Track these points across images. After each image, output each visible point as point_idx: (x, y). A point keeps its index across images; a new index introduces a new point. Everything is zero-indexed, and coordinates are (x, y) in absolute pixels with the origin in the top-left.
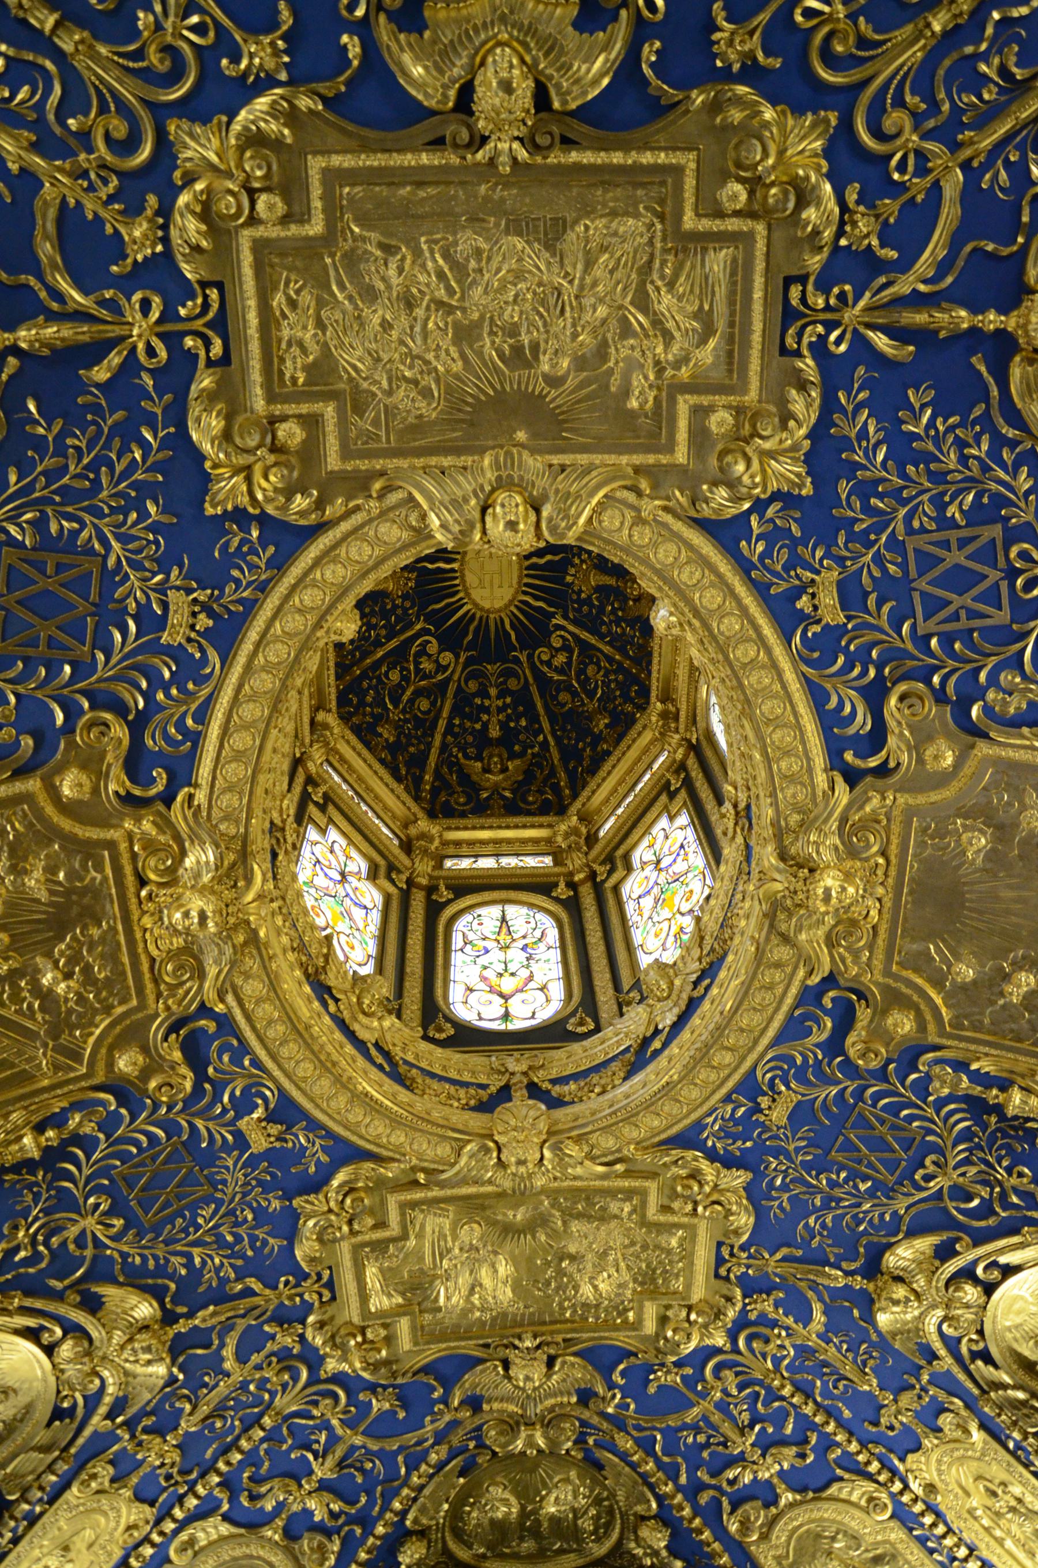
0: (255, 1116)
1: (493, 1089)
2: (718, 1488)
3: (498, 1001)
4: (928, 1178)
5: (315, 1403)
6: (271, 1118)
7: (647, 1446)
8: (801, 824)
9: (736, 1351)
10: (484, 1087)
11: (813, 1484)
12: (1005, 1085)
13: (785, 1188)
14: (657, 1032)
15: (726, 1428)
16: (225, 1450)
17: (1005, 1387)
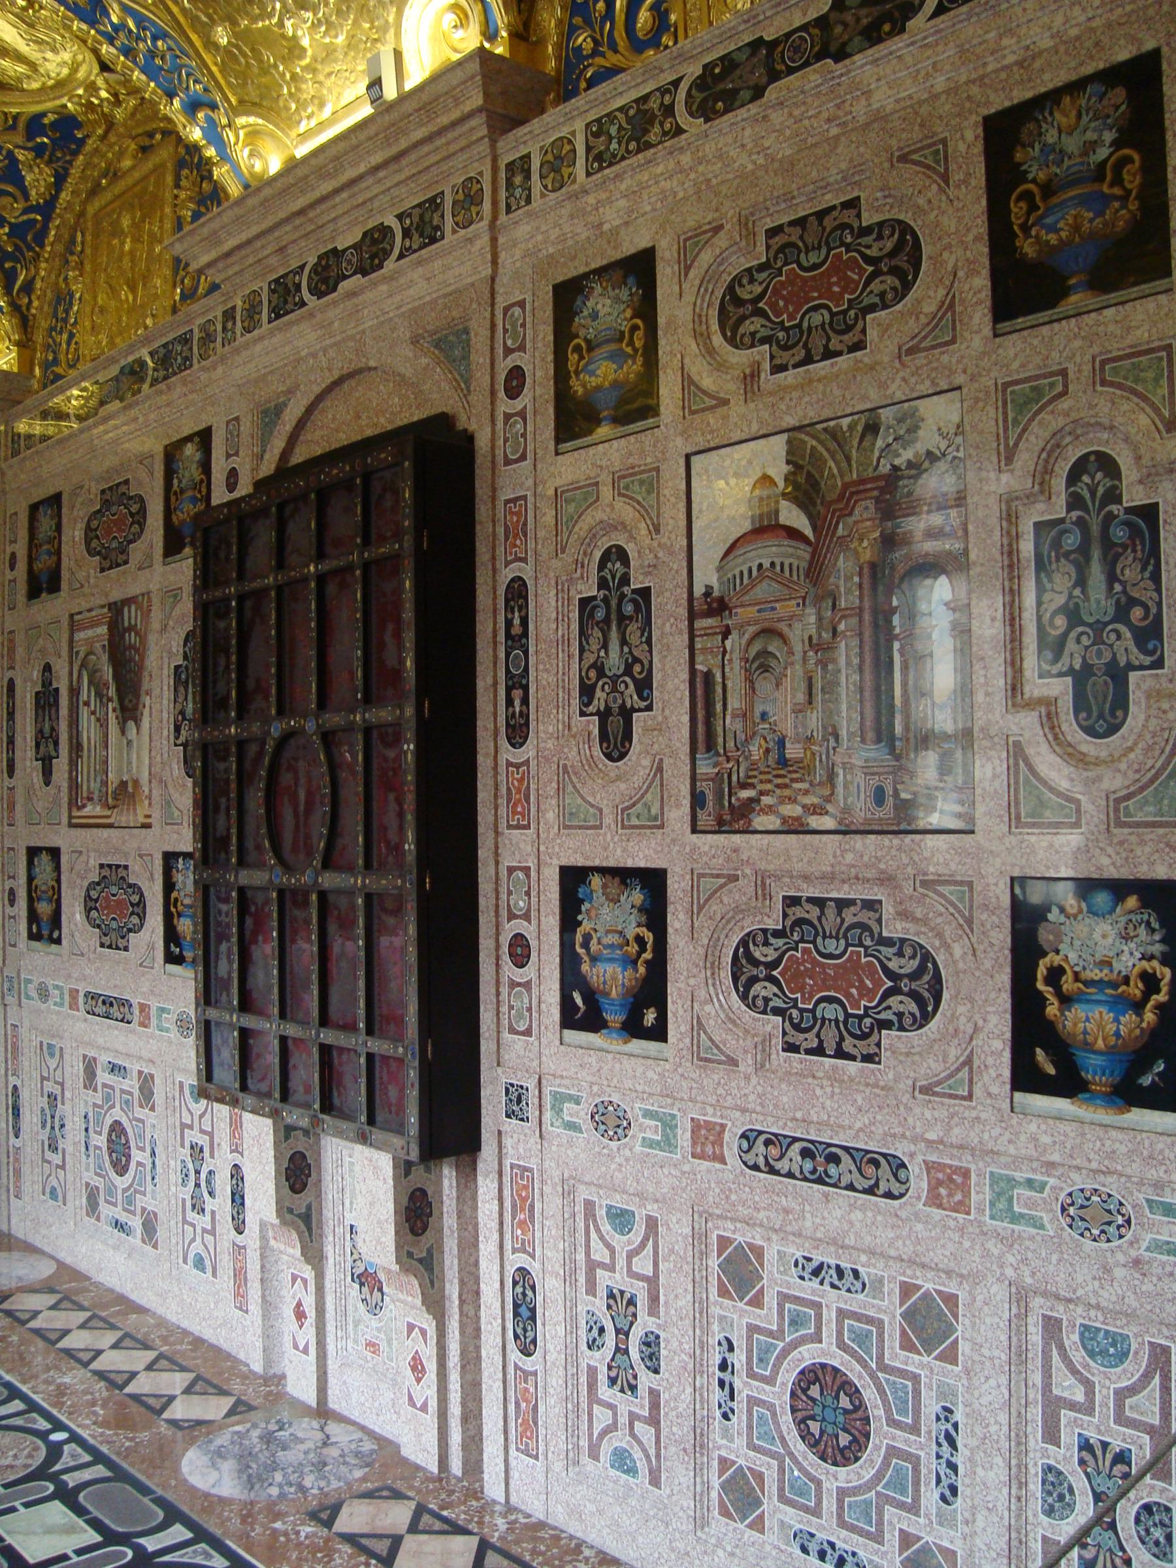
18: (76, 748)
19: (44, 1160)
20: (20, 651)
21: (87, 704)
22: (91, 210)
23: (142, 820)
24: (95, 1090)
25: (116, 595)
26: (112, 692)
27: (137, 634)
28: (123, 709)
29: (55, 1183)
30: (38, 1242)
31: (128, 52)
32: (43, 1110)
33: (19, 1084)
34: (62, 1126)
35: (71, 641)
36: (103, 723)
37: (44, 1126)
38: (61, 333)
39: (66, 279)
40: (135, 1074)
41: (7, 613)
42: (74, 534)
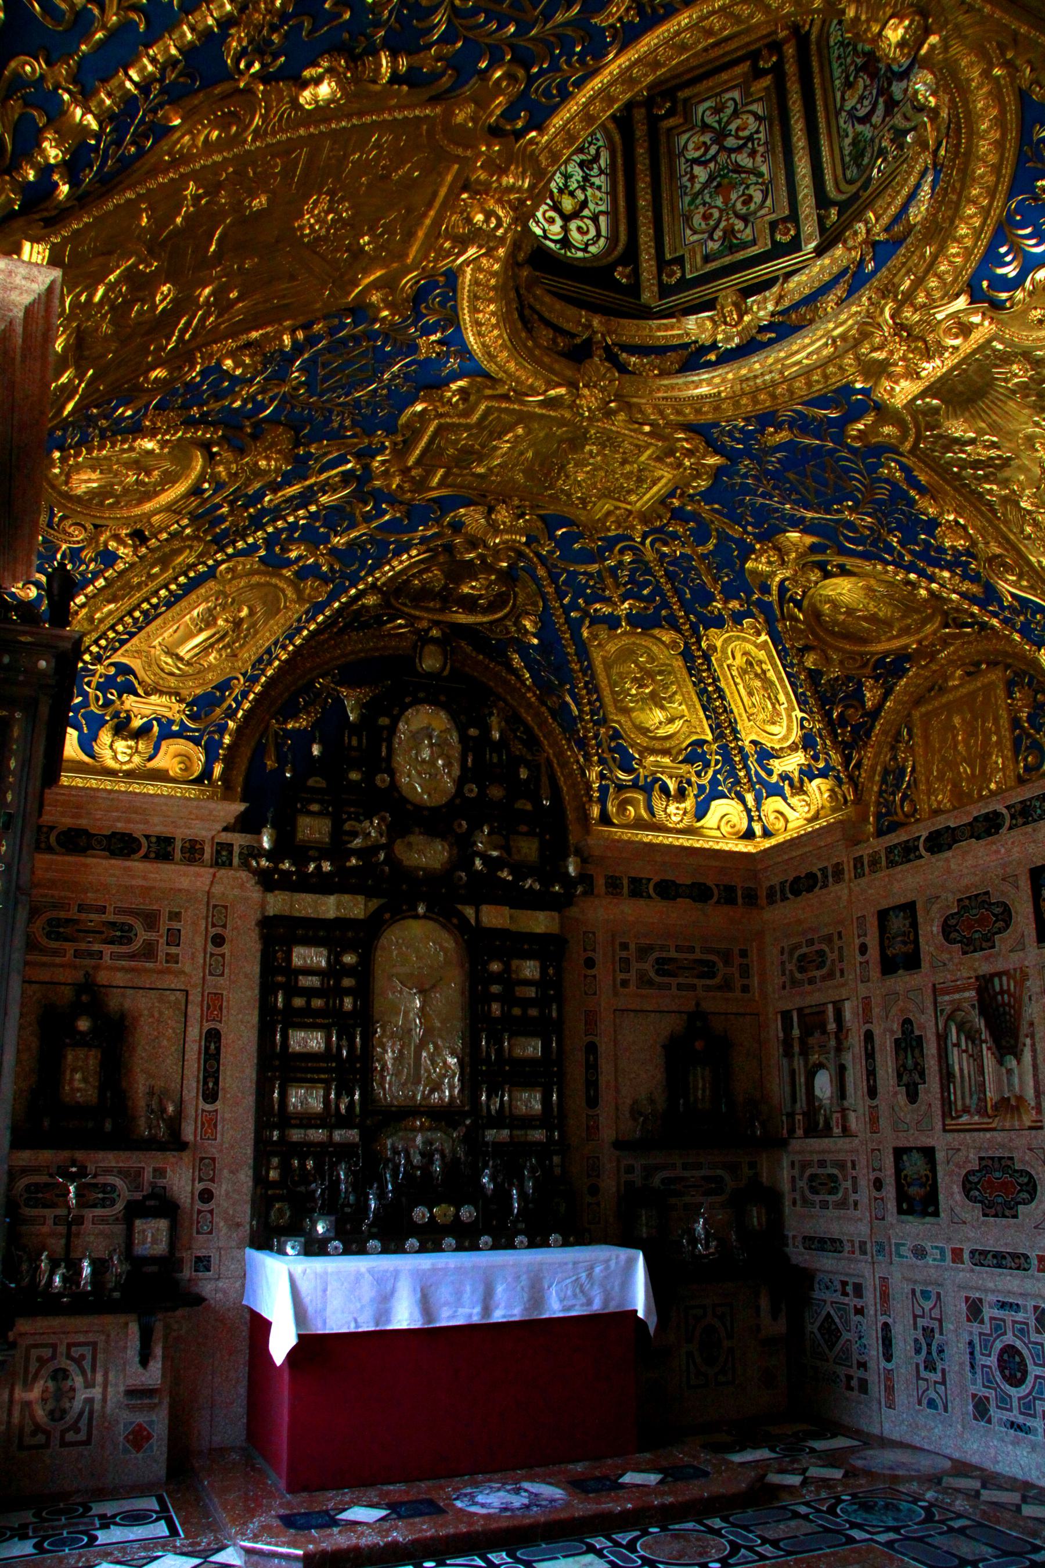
0: (433, 338)
1: (578, 341)
2: (586, 613)
3: (559, 222)
4: (838, 511)
5: (349, 503)
6: (439, 342)
7: (554, 578)
8: (924, 305)
9: (643, 543)
10: (573, 336)
11: (643, 622)
12: (922, 490)
13: (745, 476)
14: (714, 346)
15: (609, 581)
16: (274, 521)
17: (797, 620)
18: (947, 1076)
19: (919, 1377)
20: (876, 1011)
21: (958, 1045)
22: (916, 714)
23: (1028, 1124)
24: (982, 1322)
25: (985, 969)
26: (985, 1035)
27: (1010, 995)
28: (999, 1047)
29: (934, 1396)
30: (917, 1441)
31: (1005, 621)
32: (916, 1340)
33: (890, 1321)
34: (941, 1351)
35: (935, 1003)
36: (977, 1059)
37: (918, 1351)
38: (894, 794)
39: (894, 758)
40: (1030, 1309)
41: (860, 986)
42: (930, 930)
